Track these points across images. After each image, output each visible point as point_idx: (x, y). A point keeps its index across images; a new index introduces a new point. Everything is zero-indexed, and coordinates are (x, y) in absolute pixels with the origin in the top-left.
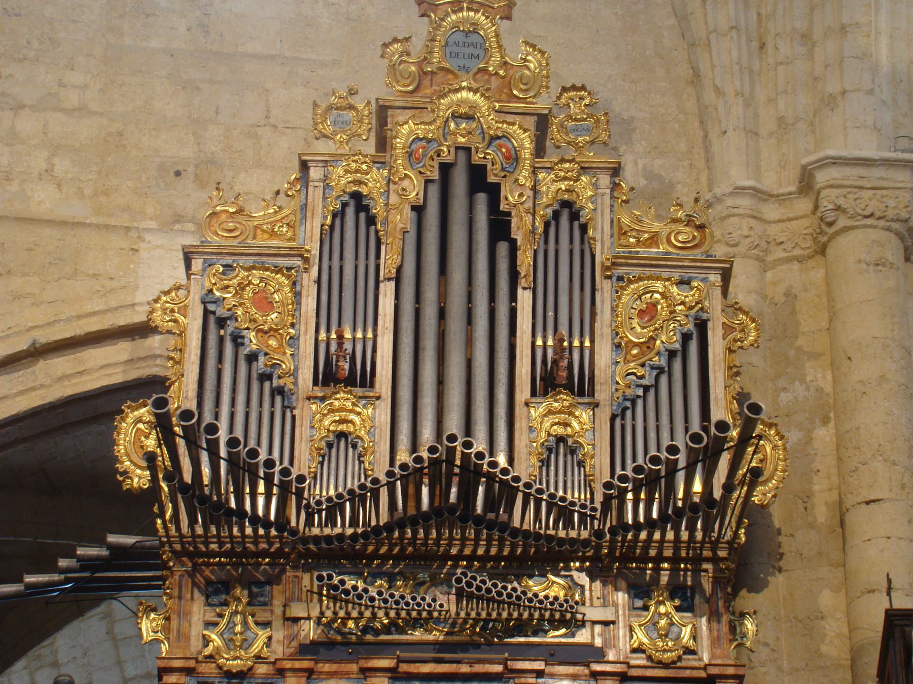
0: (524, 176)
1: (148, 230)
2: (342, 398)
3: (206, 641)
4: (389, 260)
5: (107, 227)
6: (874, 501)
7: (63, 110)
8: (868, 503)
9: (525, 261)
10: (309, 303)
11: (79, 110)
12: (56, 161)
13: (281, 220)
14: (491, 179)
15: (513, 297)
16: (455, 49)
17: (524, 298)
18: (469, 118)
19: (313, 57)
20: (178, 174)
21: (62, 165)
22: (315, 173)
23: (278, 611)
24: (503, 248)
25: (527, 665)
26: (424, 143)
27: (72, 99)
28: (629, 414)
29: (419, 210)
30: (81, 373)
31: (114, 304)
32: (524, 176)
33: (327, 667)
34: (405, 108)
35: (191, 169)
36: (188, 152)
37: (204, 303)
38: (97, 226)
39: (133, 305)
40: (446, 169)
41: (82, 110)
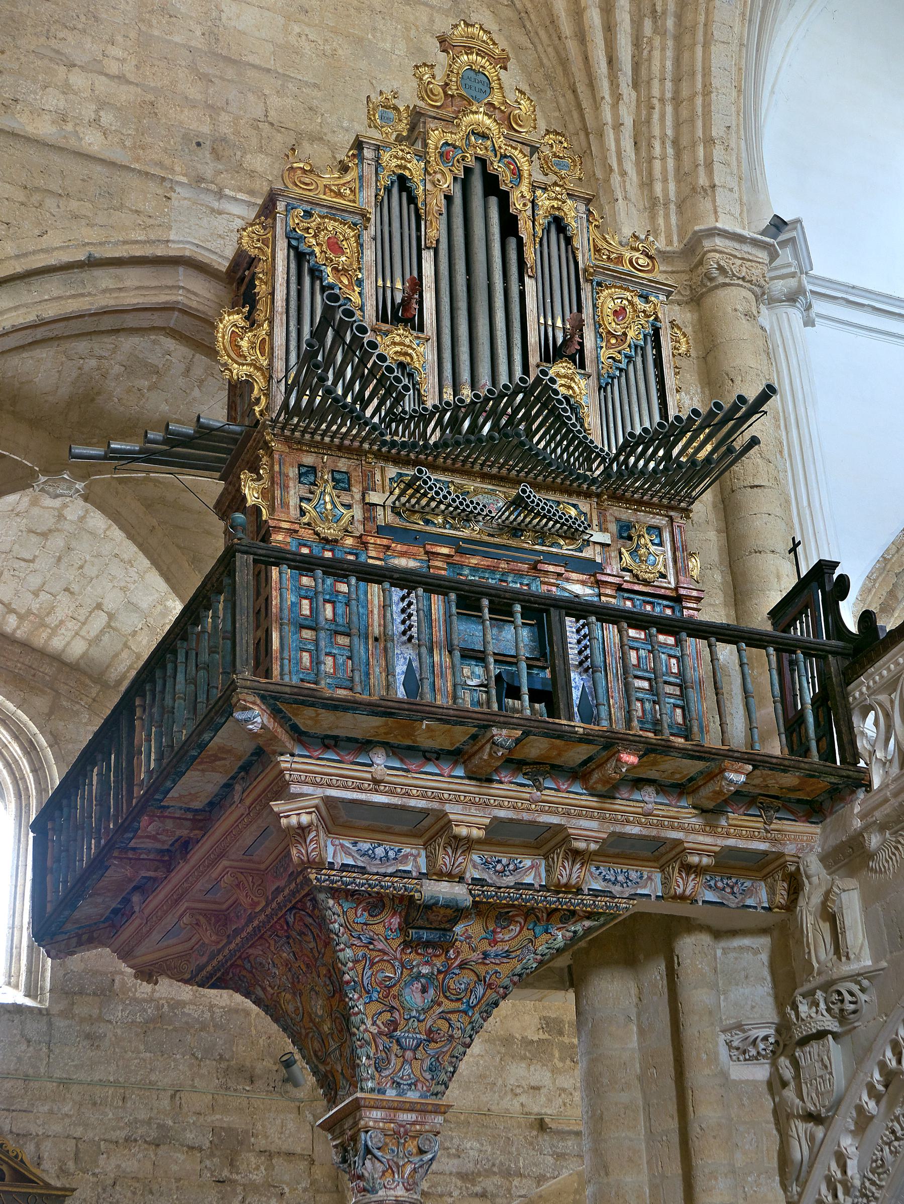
0: (525, 188)
1: (181, 184)
2: (400, 334)
3: (303, 513)
4: (435, 230)
5: (147, 174)
6: (757, 486)
7: (106, 75)
8: (752, 487)
9: (530, 255)
10: (369, 255)
11: (118, 77)
12: (102, 113)
13: (344, 185)
14: (503, 187)
15: (521, 281)
16: (468, 82)
17: (529, 283)
18: (484, 136)
19: (299, 77)
20: (199, 144)
21: (107, 118)
22: (368, 153)
23: (358, 496)
24: (512, 242)
25: (551, 568)
26: (451, 148)
27: (113, 68)
28: (609, 388)
29: (449, 199)
30: (120, 289)
31: (153, 237)
32: (525, 188)
33: (399, 547)
34: (435, 118)
35: (208, 143)
36: (206, 129)
37: (288, 238)
38: (139, 171)
39: (168, 241)
40: (468, 171)
41: (121, 78)
